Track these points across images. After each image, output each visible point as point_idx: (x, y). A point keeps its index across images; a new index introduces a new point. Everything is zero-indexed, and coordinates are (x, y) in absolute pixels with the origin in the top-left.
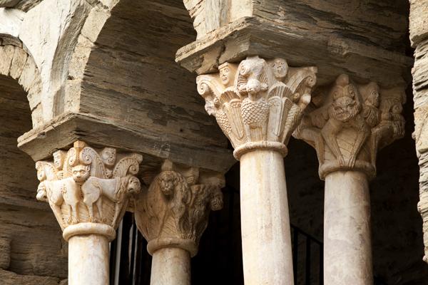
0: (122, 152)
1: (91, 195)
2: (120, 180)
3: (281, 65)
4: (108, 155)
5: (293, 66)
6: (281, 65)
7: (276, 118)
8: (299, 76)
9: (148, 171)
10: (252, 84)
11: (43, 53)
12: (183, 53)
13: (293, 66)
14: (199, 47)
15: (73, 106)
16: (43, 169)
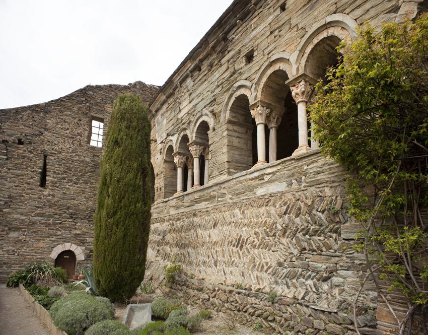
0: (184, 156)
1: (180, 162)
2: (184, 160)
3: (199, 146)
4: (182, 156)
5: (200, 146)
6: (199, 146)
7: (198, 153)
8: (201, 147)
9: (187, 159)
10: (195, 149)
11: (174, 142)
12: (188, 144)
13: (200, 146)
14: (189, 143)
15: (177, 150)
16: (175, 158)
